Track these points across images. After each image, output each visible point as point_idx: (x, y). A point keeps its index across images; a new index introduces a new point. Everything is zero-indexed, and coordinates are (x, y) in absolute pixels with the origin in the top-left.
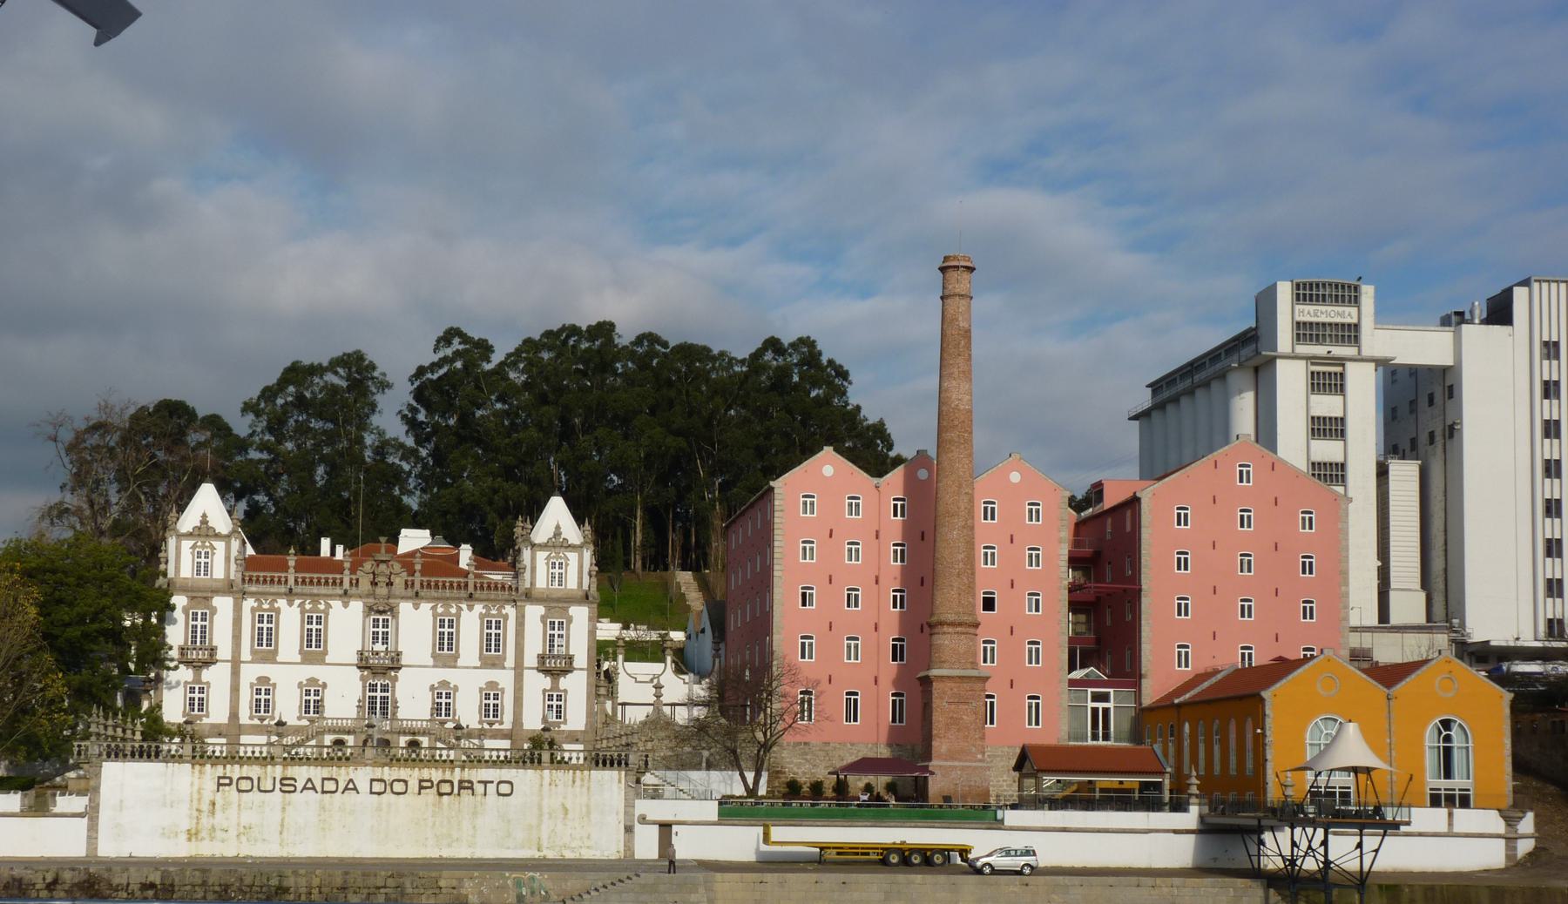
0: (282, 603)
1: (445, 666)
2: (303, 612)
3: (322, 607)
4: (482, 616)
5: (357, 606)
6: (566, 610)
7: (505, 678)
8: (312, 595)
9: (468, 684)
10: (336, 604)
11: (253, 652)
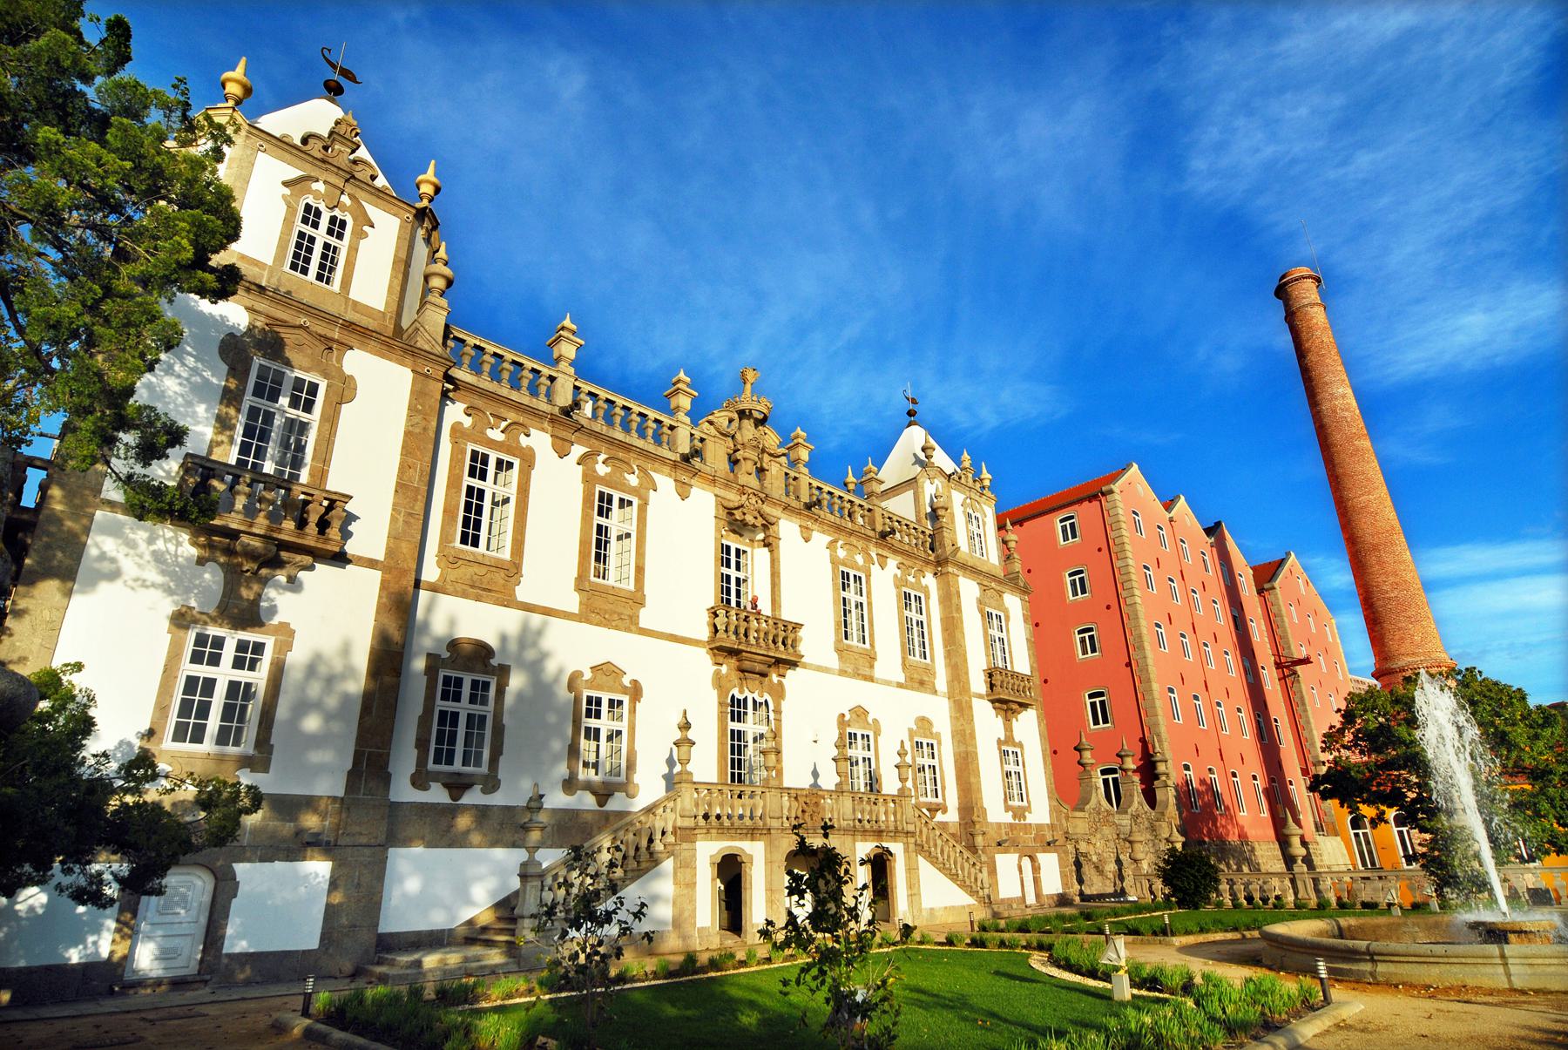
0: (539, 440)
1: (857, 675)
2: (589, 479)
3: (633, 480)
4: (899, 583)
5: (704, 501)
6: (1000, 593)
7: (938, 710)
8: (612, 442)
9: (896, 713)
10: (665, 482)
11: (449, 560)
